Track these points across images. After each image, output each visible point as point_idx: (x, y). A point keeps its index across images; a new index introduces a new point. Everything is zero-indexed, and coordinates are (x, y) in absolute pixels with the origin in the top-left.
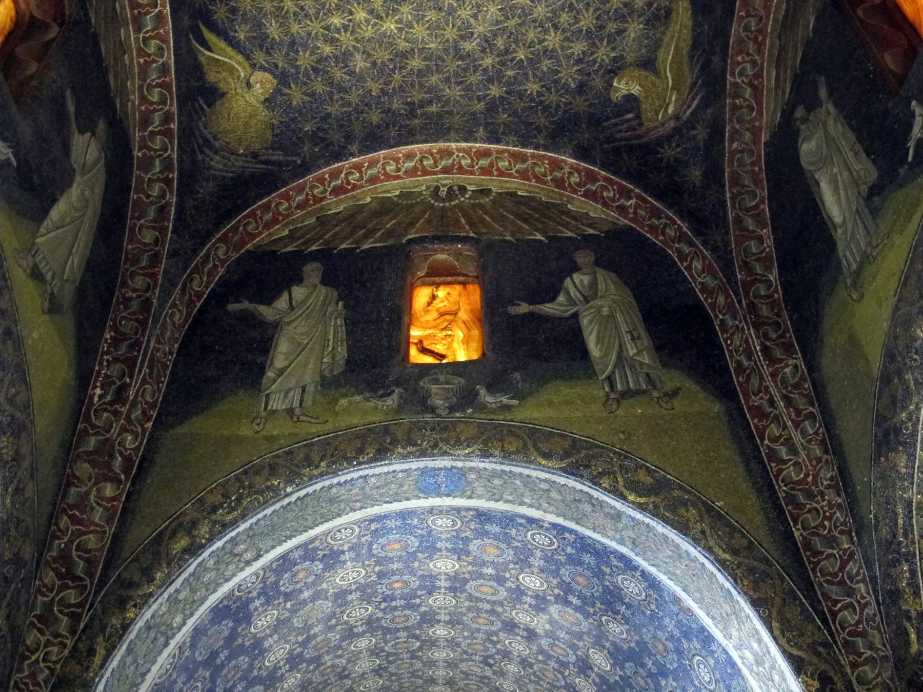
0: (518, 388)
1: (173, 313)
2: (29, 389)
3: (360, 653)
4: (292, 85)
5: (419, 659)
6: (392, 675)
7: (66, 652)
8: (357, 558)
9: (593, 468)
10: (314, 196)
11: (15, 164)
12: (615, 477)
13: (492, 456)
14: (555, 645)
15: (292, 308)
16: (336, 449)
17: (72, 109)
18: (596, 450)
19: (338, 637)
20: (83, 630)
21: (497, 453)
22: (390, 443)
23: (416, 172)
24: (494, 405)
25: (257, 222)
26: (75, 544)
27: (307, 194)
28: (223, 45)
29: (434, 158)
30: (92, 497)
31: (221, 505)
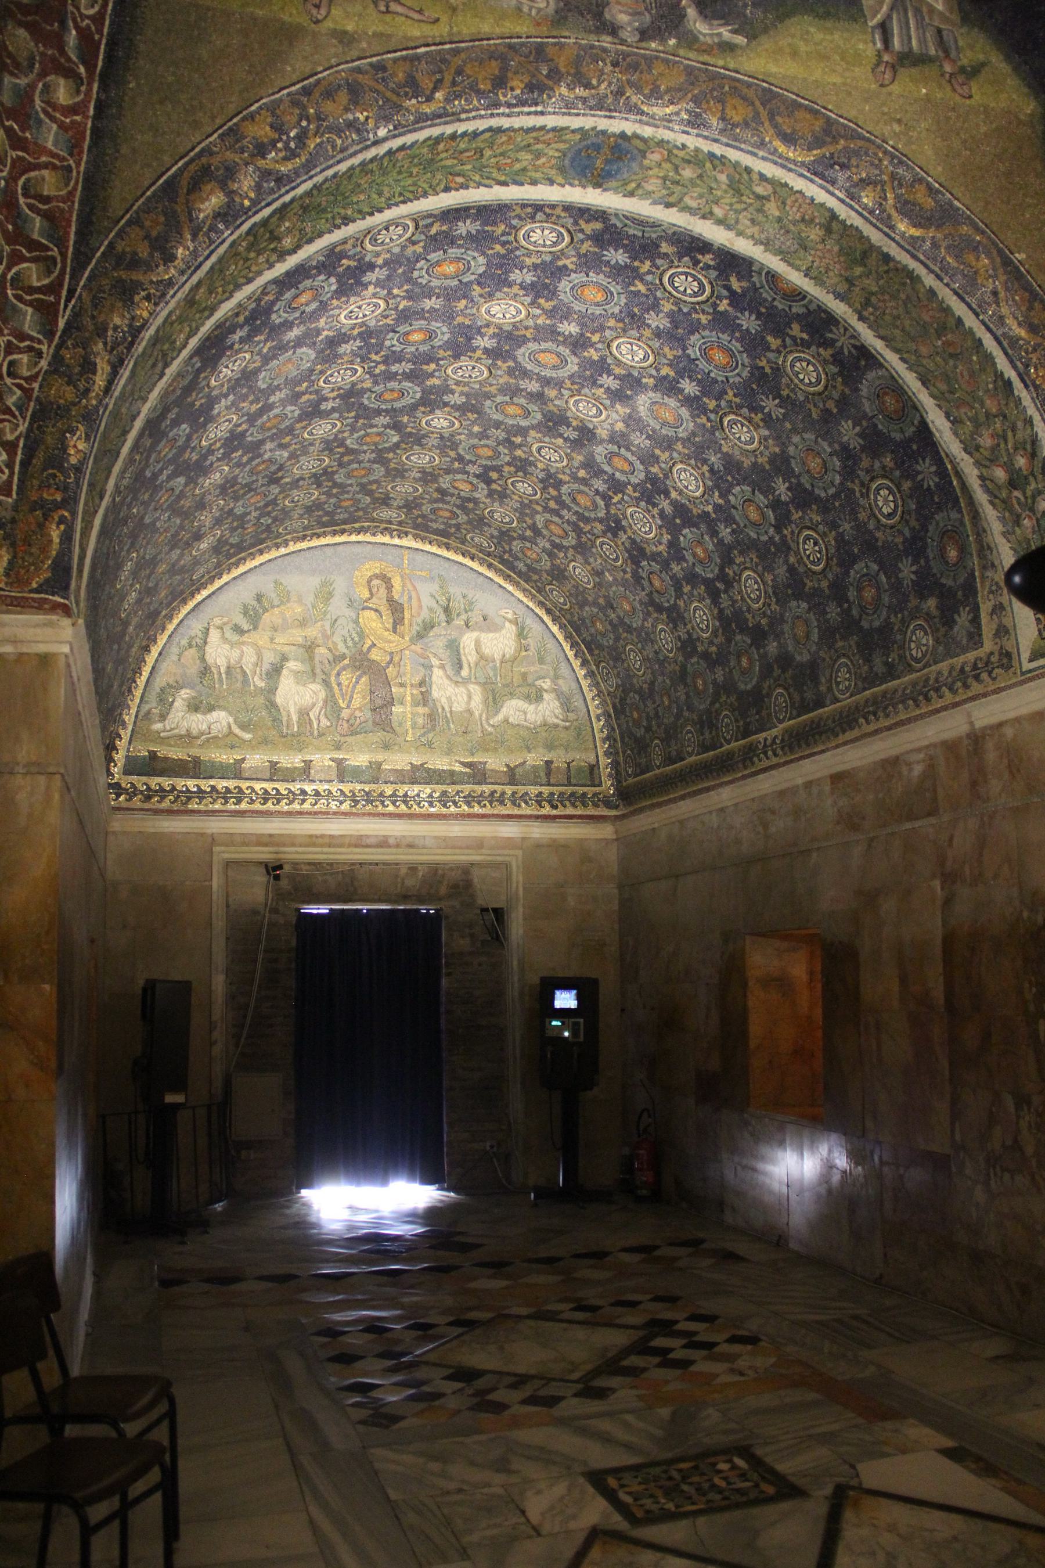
0: (745, 16)
6: (335, 485)
7: (44, 364)
9: (854, 170)
12: (884, 191)
13: (706, 125)
14: (618, 455)
16: (459, 72)
18: (860, 143)
19: (297, 412)
20: (64, 332)
21: (714, 121)
22: (548, 76)
24: (709, 40)
26: (21, 182)
30: (38, 102)
31: (273, 143)
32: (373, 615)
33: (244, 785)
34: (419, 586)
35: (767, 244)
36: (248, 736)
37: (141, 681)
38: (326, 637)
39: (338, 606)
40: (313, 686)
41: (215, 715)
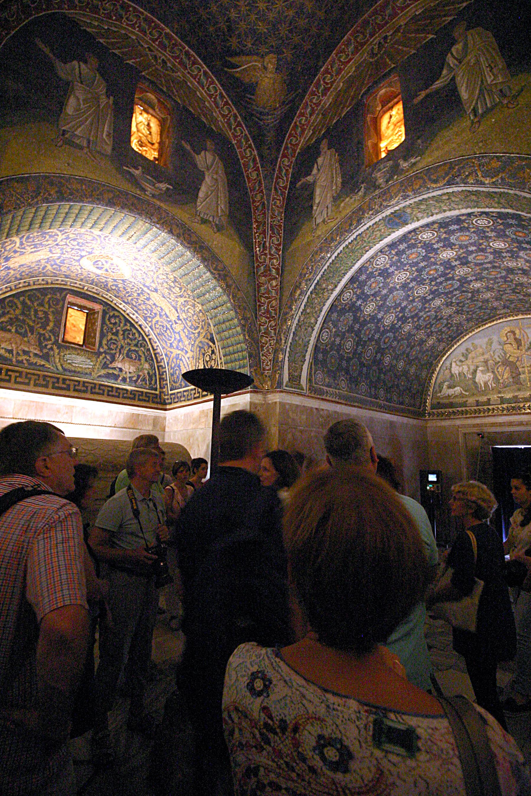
1: (276, 202)
2: (222, 262)
3: (439, 307)
4: (284, 50)
5: (477, 301)
8: (398, 269)
10: (315, 104)
11: (171, 187)
13: (408, 196)
15: (319, 170)
17: (188, 148)
21: (410, 194)
23: (357, 48)
25: (295, 137)
27: (311, 106)
28: (244, 58)
29: (361, 33)
32: (509, 345)
33: (467, 408)
34: (526, 331)
35: (466, 208)
36: (467, 393)
37: (433, 382)
38: (491, 357)
39: (495, 346)
40: (489, 374)
41: (456, 389)
